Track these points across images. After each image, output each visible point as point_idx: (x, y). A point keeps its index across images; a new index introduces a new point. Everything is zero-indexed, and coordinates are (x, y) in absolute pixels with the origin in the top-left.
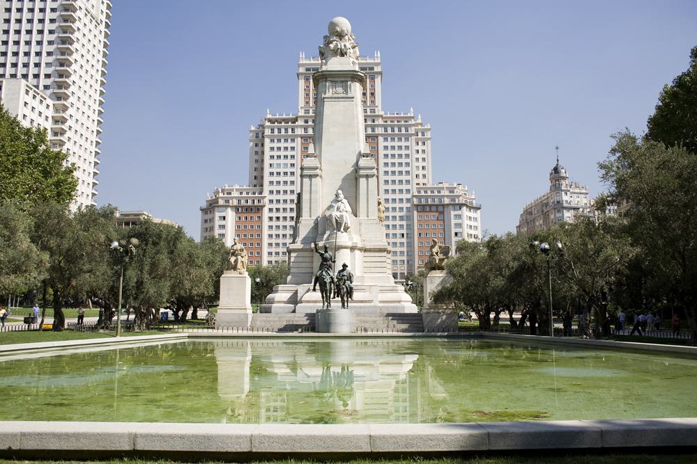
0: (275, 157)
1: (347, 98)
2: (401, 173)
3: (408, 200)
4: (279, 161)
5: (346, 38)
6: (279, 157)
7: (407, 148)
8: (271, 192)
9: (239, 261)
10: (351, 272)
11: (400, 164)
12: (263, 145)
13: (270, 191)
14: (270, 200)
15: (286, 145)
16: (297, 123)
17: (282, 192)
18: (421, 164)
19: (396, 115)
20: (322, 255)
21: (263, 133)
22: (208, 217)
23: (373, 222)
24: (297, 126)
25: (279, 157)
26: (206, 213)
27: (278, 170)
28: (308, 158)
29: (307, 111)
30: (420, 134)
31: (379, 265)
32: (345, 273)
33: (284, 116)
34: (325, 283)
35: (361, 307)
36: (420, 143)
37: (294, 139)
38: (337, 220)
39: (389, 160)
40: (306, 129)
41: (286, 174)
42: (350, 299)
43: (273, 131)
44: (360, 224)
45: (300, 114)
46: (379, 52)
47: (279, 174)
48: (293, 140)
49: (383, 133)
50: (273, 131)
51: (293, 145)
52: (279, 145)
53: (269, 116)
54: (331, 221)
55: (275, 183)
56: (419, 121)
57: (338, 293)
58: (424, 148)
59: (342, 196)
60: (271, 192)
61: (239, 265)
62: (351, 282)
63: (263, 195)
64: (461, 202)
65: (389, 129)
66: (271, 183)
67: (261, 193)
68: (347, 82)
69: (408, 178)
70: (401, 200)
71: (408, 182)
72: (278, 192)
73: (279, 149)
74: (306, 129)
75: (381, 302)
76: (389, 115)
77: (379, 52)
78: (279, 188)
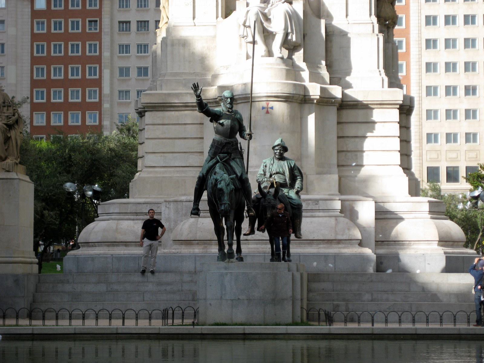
34: (221, 190)
42: (293, 236)
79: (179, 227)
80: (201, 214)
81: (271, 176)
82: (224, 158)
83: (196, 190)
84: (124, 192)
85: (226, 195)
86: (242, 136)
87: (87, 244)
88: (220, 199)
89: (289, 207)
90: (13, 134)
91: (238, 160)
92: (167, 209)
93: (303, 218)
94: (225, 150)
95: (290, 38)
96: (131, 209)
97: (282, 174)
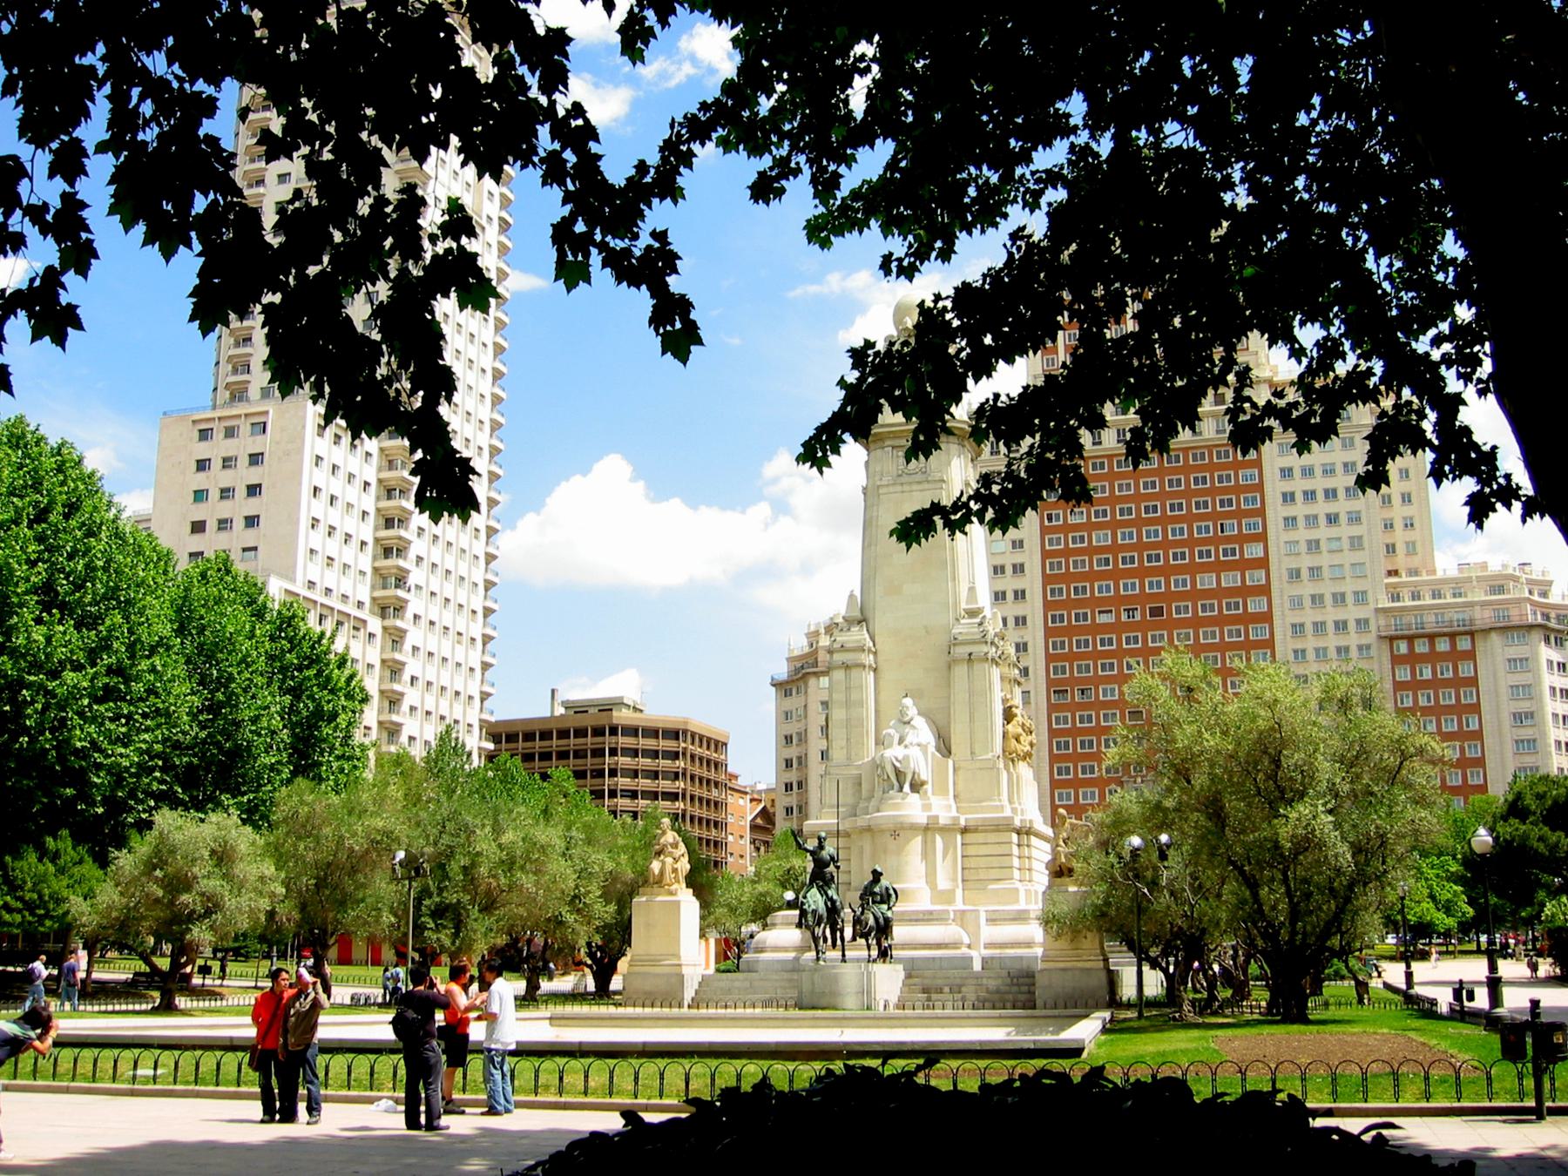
1: (928, 482)
3: (1362, 624)
9: (668, 869)
20: (812, 853)
22: (794, 702)
26: (787, 694)
31: (995, 861)
32: (877, 889)
39: (1300, 509)
54: (883, 768)
57: (861, 932)
59: (912, 711)
61: (669, 876)
64: (1530, 620)
70: (1341, 626)
75: (988, 946)
89: (881, 920)
90: (678, 865)
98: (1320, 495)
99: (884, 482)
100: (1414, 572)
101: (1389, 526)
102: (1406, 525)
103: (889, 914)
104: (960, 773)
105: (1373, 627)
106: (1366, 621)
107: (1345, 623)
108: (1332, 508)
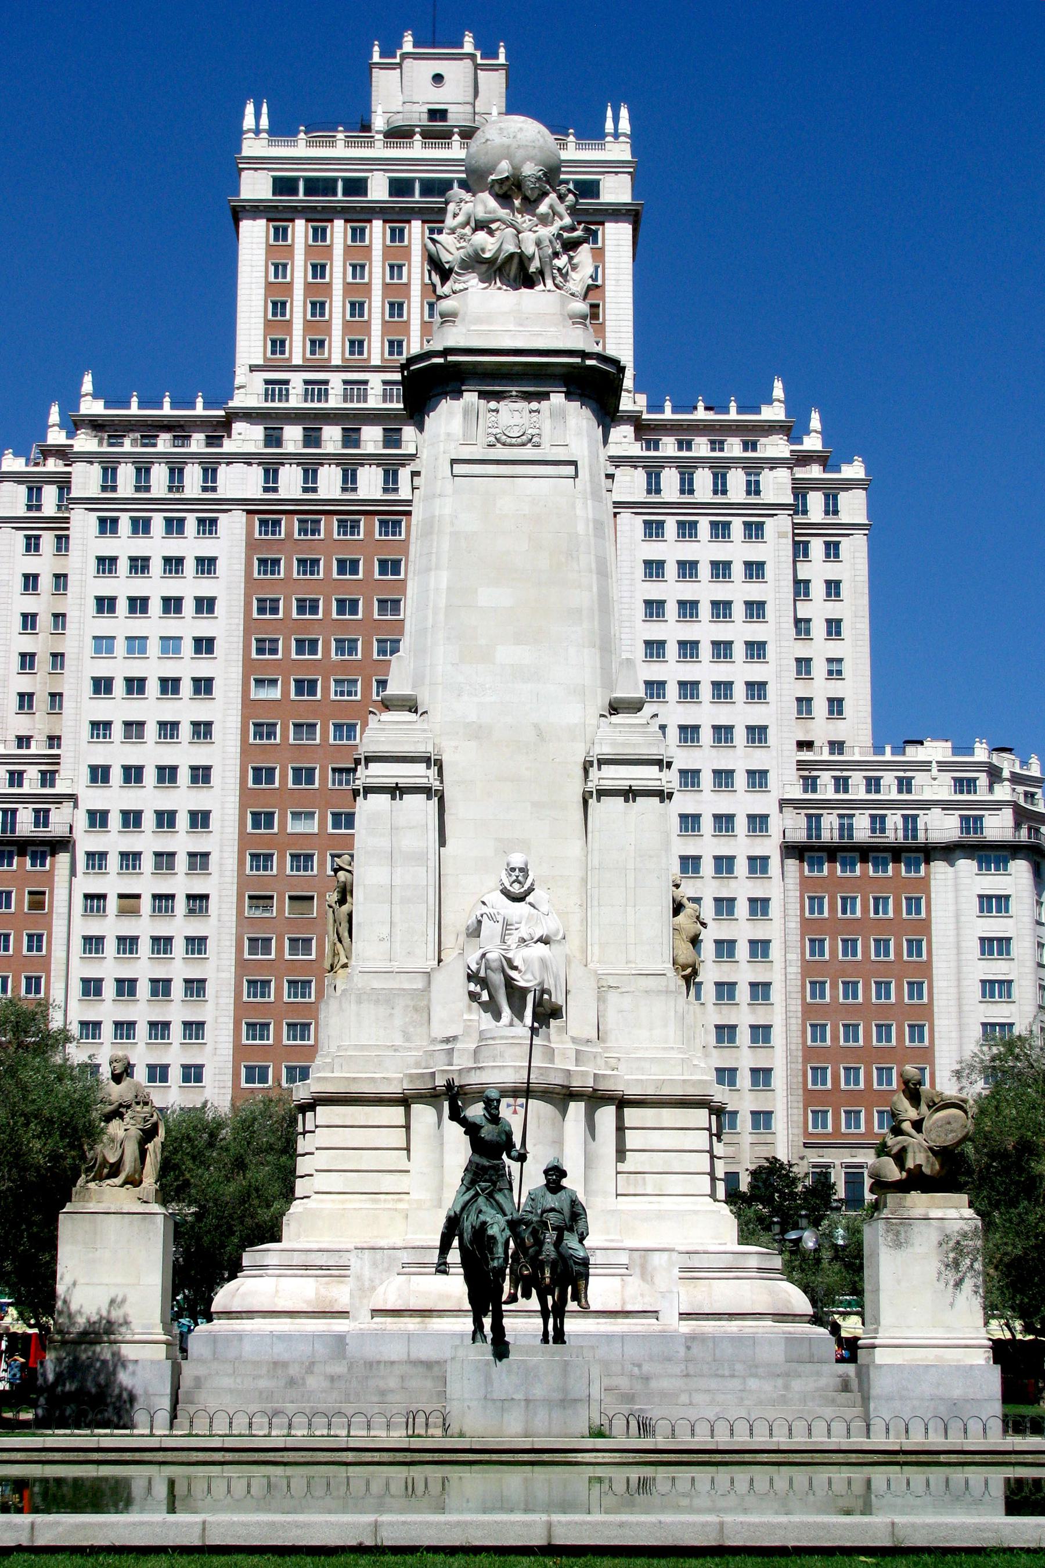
0: (122, 606)
2: (722, 690)
3: (758, 822)
4: (138, 626)
5: (543, 208)
6: (138, 605)
7: (755, 570)
8: (99, 774)
10: (581, 1197)
11: (722, 649)
12: (62, 542)
13: (94, 769)
14: (91, 814)
15: (174, 547)
16: (228, 446)
17: (150, 776)
18: (819, 648)
19: (701, 414)
20: (472, 1129)
21: (64, 484)
23: (651, 983)
24: (232, 458)
25: (138, 605)
27: (136, 669)
28: (387, 716)
29: (276, 388)
30: (816, 501)
31: (677, 1162)
33: (167, 410)
34: (493, 1237)
35: (609, 1337)
36: (817, 547)
37: (214, 522)
38: (509, 982)
40: (271, 474)
41: (170, 686)
42: (572, 1306)
43: (110, 472)
44: (601, 999)
45: (239, 401)
46: (624, 113)
47: (136, 685)
48: (208, 526)
49: (641, 496)
50: (110, 472)
51: (206, 548)
52: (140, 547)
53: (92, 407)
55: (118, 730)
56: (812, 443)
58: (832, 571)
60: (99, 774)
62: (581, 1241)
63: (61, 787)
65: (670, 478)
66: (100, 728)
67: (48, 778)
68: (545, 396)
69: (757, 714)
71: (757, 734)
72: (133, 774)
73: (140, 565)
74: (271, 474)
75: (685, 1316)
76: (668, 414)
77: (624, 113)
78: (133, 755)
79: (381, 1290)
80: (452, 1270)
81: (543, 1212)
82: (486, 1189)
83: (443, 1235)
84: (272, 1233)
85: (500, 1245)
86: (509, 1156)
87: (229, 1314)
88: (492, 1253)
90: (150, 1146)
91: (506, 1191)
92: (359, 1261)
93: (591, 1278)
94: (487, 1177)
95: (546, 996)
96: (297, 1259)
97: (559, 1212)
98: (705, 610)
99: (466, 453)
100: (837, 746)
101: (804, 665)
102: (830, 672)
103: (581, 1254)
104: (612, 997)
105: (775, 824)
106: (764, 818)
107: (730, 818)
108: (722, 632)
